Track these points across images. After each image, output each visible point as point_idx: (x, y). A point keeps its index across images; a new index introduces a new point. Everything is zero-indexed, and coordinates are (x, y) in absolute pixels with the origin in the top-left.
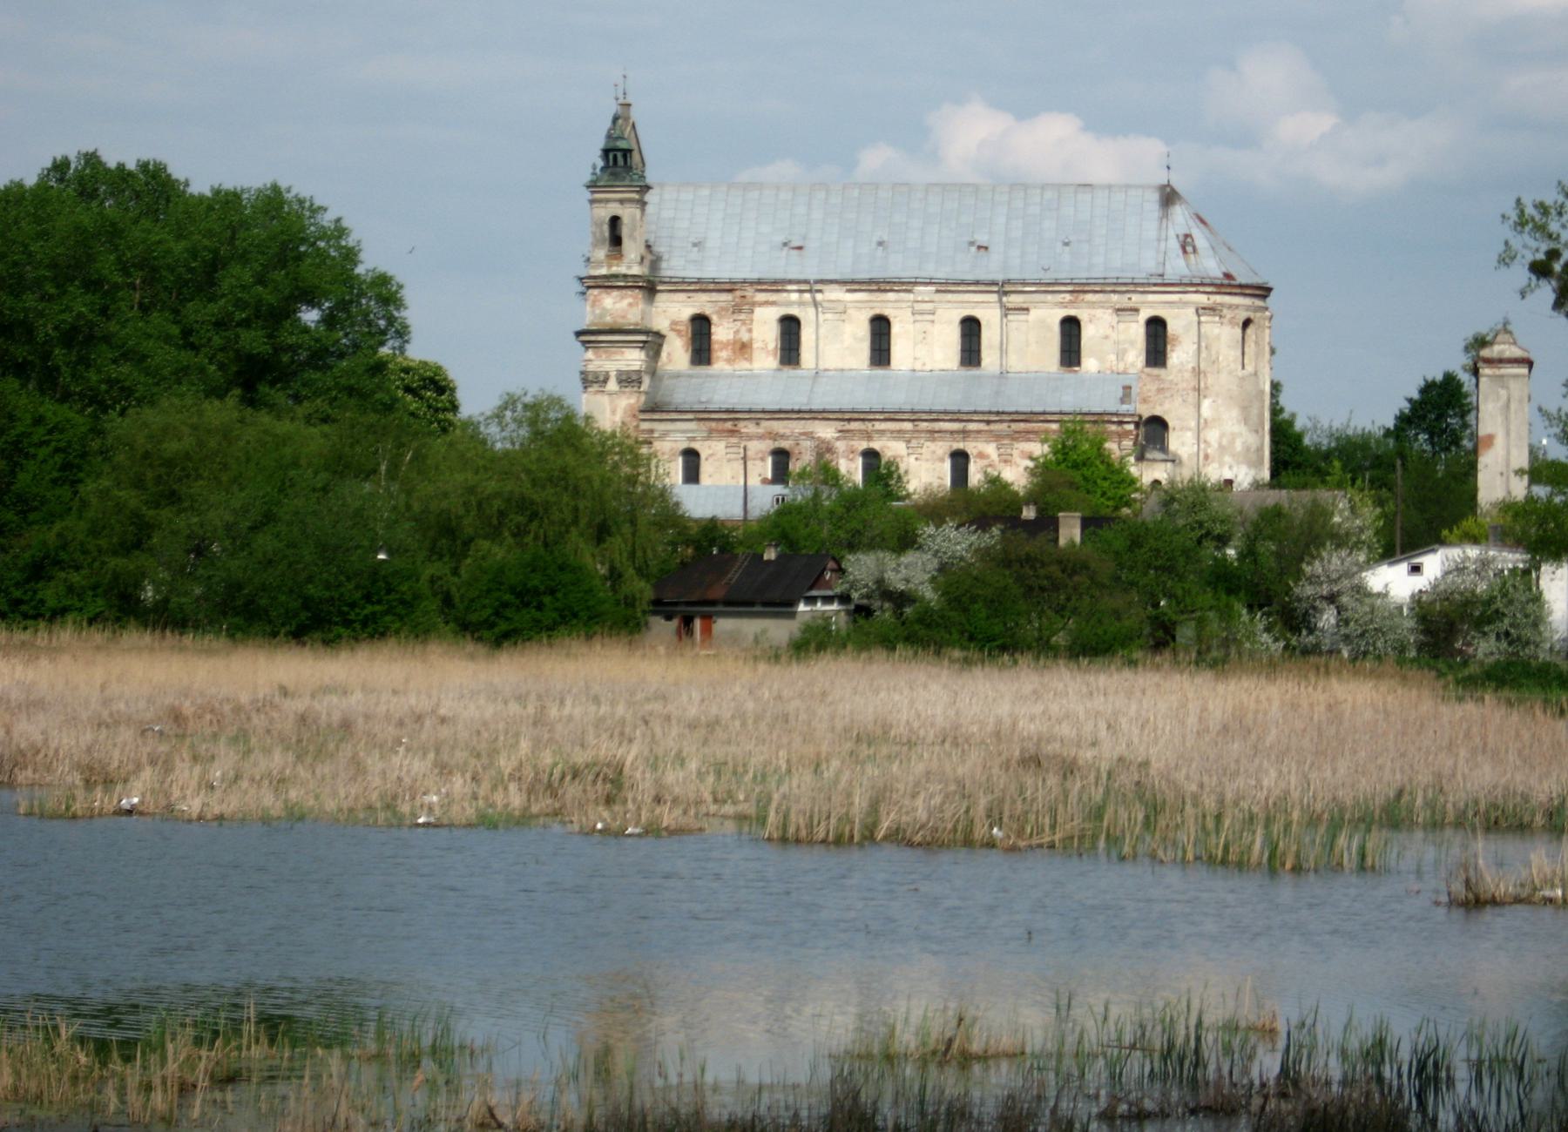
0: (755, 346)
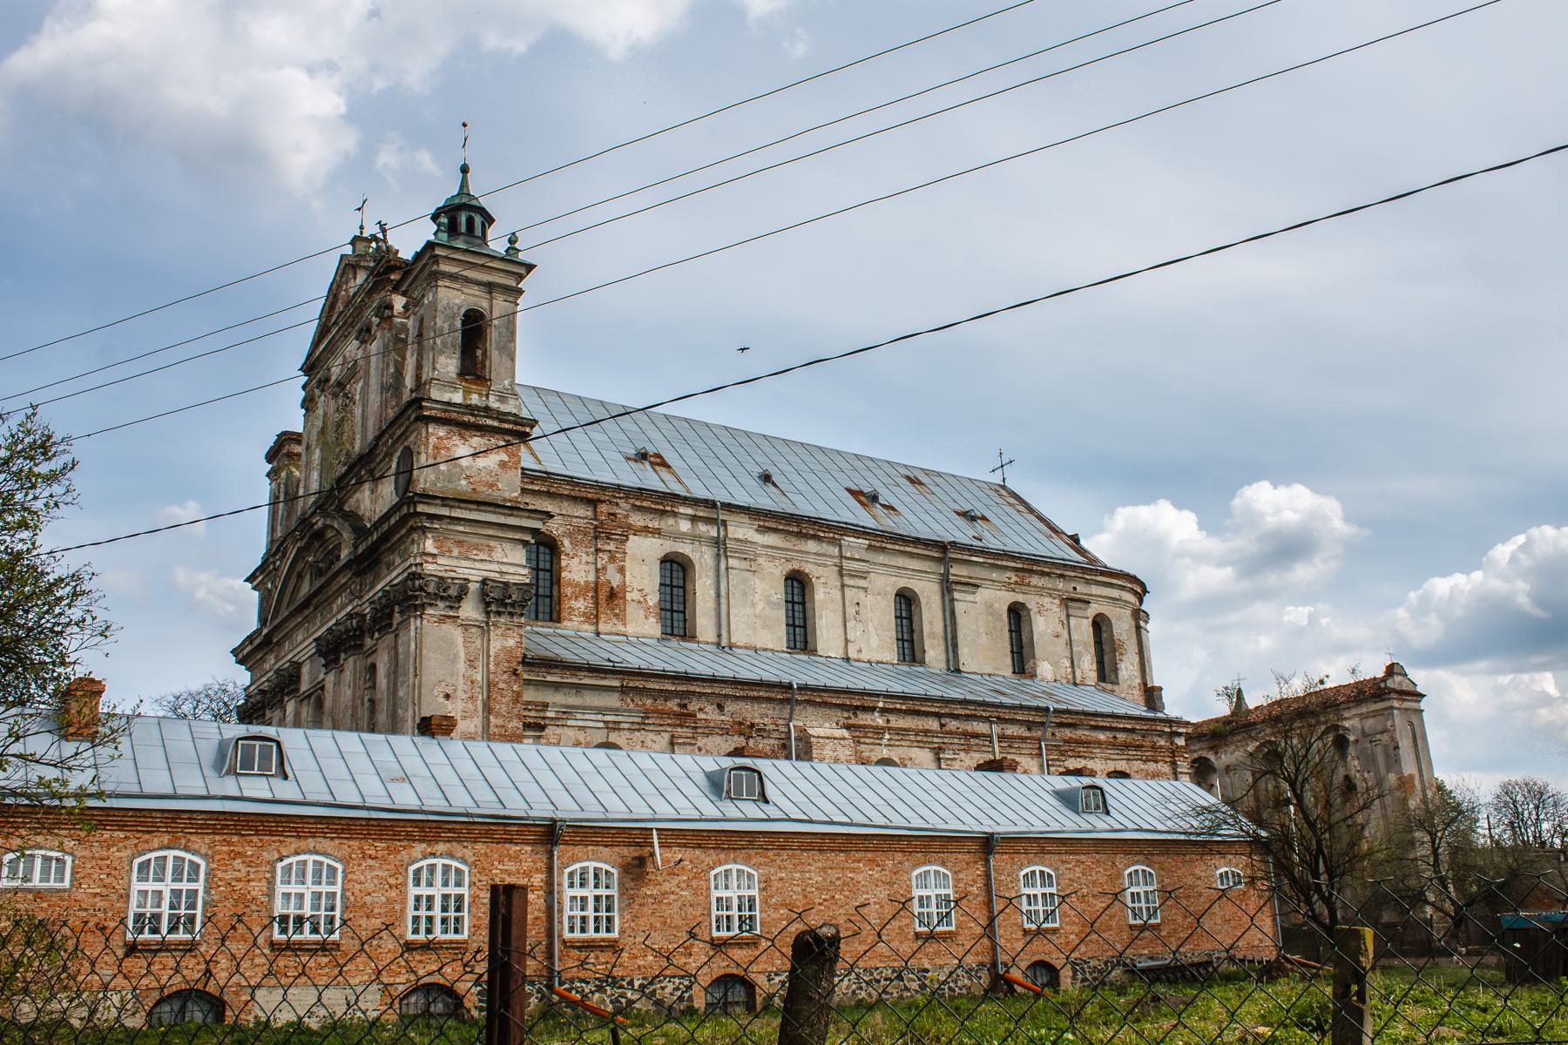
0: (629, 596)
